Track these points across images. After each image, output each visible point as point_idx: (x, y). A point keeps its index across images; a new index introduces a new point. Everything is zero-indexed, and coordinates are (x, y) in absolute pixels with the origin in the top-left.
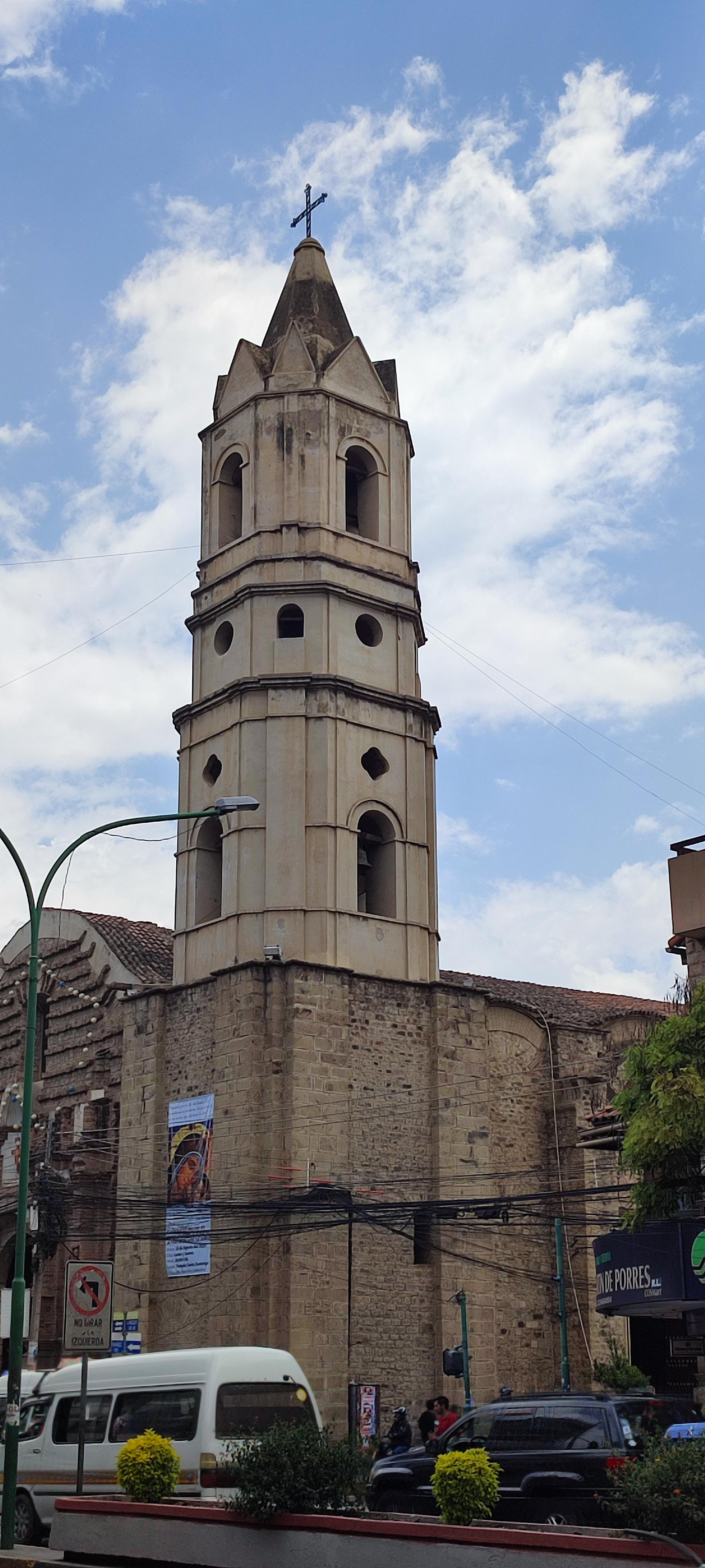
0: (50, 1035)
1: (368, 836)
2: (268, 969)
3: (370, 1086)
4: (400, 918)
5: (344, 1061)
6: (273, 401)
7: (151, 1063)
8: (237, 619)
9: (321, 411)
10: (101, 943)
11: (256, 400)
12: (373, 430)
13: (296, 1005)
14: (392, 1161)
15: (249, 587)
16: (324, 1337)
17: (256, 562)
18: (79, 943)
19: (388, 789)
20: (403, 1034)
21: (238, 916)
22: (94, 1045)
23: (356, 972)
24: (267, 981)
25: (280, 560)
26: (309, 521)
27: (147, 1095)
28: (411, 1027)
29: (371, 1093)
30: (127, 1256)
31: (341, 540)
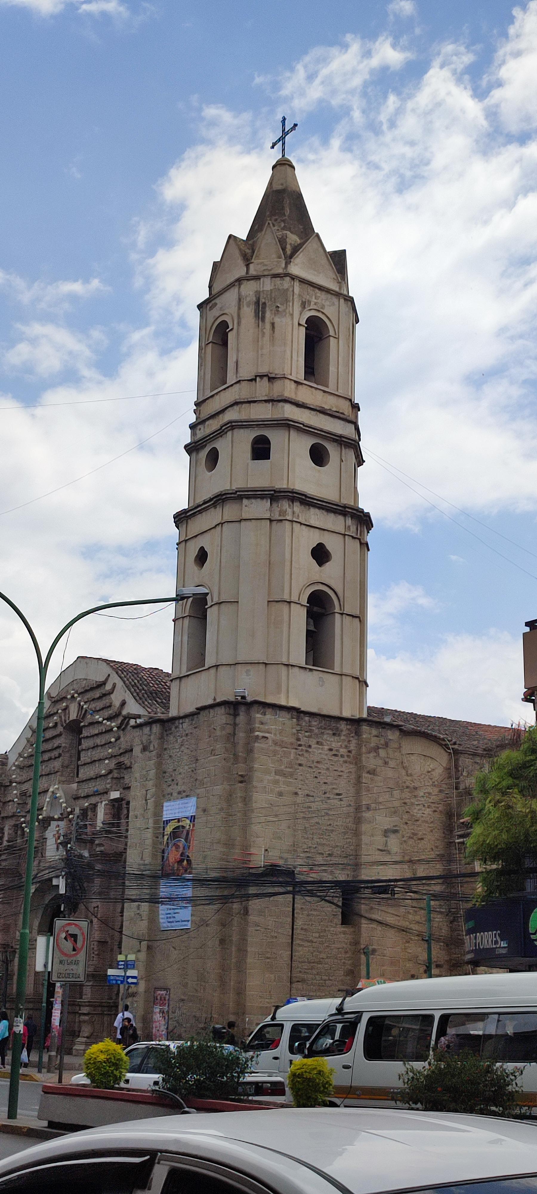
0: (83, 750)
1: (315, 609)
2: (237, 706)
3: (311, 794)
4: (337, 670)
5: (291, 775)
6: (252, 282)
7: (152, 773)
8: (222, 445)
9: (287, 289)
10: (120, 684)
11: (239, 281)
12: (328, 303)
13: (257, 733)
14: (326, 849)
15: (230, 422)
16: (272, 976)
17: (236, 403)
18: (104, 683)
19: (330, 574)
21: (217, 666)
22: (113, 758)
23: (302, 709)
24: (236, 715)
25: (255, 402)
26: (276, 372)
27: (149, 796)
28: (343, 751)
29: (311, 799)
30: (132, 914)
31: (300, 387)
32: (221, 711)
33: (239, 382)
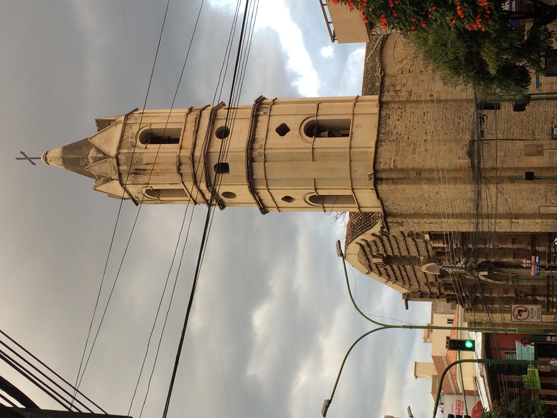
1: (315, 131)
2: (377, 179)
3: (424, 131)
4: (350, 117)
5: (415, 144)
7: (415, 220)
9: (126, 156)
10: (361, 237)
12: (130, 131)
13: (392, 167)
14: (456, 121)
18: (361, 245)
19: (294, 123)
20: (401, 116)
23: (376, 139)
24: (382, 179)
26: (176, 161)
28: (399, 112)
29: (428, 130)
31: (183, 146)
32: (379, 187)
33: (183, 183)
